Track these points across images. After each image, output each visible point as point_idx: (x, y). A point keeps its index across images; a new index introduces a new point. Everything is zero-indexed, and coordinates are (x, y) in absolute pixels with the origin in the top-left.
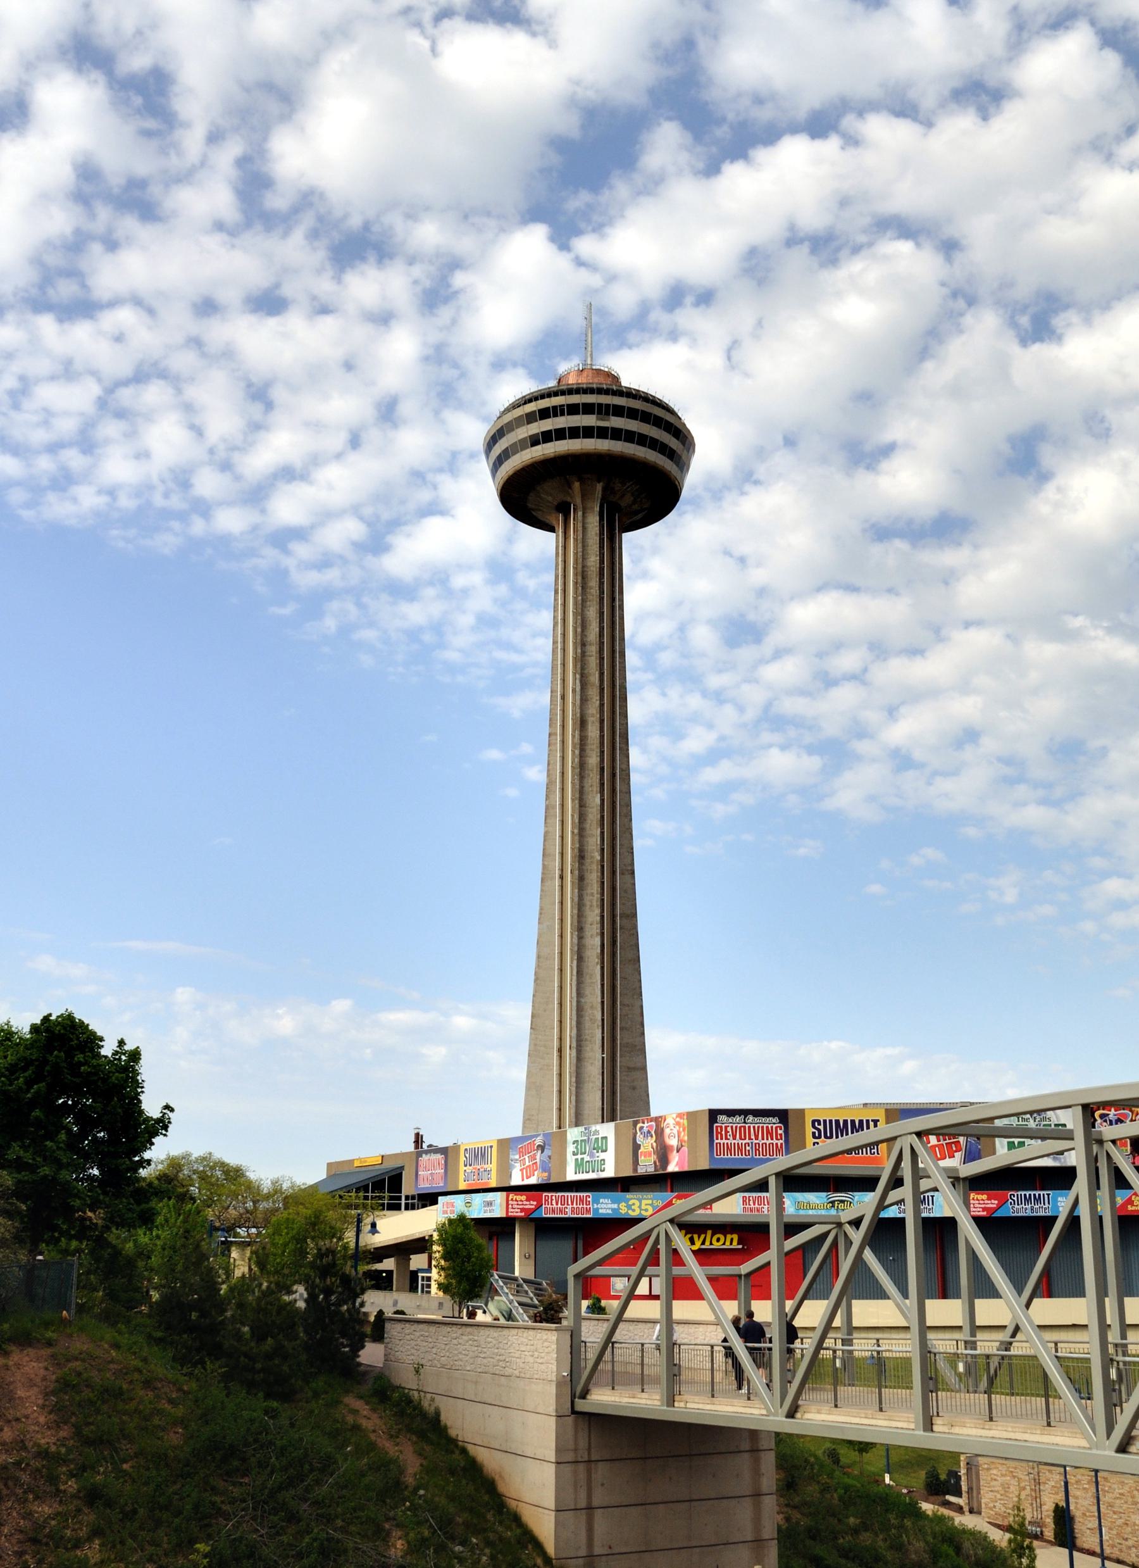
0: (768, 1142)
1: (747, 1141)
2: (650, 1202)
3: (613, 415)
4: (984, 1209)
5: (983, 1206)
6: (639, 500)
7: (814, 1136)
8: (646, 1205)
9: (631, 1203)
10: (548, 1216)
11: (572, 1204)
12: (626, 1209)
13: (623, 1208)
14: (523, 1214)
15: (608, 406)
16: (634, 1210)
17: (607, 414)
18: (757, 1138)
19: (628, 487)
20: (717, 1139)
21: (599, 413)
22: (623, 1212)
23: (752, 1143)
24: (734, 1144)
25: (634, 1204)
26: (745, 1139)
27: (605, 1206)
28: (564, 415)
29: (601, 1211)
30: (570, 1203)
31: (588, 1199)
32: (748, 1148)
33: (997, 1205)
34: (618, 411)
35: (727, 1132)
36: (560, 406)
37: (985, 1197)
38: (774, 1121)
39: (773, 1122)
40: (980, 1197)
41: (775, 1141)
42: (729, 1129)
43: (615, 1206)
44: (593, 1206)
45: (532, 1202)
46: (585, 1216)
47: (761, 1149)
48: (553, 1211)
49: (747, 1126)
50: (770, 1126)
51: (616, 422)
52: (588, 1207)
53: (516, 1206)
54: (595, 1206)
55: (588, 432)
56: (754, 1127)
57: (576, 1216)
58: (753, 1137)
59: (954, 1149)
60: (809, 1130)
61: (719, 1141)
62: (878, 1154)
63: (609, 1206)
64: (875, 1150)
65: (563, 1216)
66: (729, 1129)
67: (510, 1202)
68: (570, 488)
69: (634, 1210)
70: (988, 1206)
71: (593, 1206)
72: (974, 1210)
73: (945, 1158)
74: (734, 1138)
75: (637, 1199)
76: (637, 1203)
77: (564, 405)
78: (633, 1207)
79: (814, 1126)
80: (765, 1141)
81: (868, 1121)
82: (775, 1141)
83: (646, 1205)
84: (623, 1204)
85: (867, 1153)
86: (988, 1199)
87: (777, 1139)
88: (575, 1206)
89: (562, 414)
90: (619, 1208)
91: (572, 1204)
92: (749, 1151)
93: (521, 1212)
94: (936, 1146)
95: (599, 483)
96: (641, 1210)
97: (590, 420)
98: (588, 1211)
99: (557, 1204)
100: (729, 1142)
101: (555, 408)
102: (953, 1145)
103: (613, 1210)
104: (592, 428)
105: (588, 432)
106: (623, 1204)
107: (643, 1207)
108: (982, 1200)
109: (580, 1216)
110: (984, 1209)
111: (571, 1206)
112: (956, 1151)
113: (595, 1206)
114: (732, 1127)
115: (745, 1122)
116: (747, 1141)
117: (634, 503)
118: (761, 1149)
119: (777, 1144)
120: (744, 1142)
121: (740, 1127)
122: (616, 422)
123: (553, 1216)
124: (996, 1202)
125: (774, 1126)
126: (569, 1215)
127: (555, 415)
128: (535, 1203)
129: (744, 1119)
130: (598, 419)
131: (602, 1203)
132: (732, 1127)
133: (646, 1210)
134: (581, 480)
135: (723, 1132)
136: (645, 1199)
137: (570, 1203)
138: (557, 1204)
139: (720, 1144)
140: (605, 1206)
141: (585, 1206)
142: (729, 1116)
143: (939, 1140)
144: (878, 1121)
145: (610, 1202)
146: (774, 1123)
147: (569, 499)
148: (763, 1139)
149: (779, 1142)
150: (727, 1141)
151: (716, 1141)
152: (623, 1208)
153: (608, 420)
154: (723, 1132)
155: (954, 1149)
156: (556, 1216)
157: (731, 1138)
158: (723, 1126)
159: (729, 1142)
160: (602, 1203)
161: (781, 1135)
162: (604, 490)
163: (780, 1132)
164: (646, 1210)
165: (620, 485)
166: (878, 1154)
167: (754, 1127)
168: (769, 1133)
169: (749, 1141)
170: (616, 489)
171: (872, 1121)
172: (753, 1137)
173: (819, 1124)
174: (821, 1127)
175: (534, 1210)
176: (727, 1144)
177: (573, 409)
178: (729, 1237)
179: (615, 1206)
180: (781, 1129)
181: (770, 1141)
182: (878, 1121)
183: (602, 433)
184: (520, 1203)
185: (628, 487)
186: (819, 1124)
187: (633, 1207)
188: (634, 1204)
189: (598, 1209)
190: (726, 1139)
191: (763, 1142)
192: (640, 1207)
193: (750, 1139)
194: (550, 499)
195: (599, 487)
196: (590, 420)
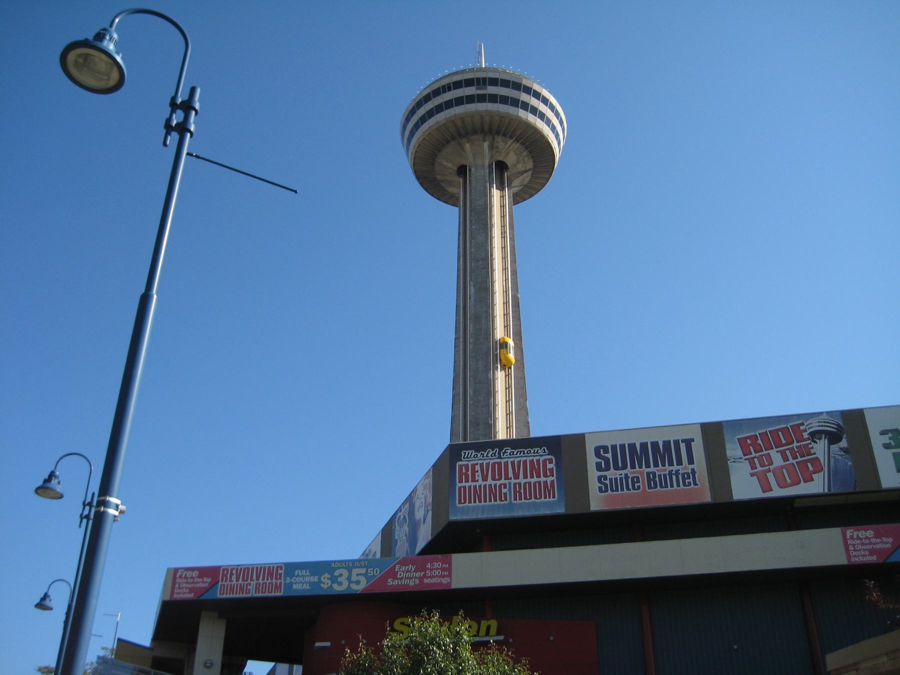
0: (533, 481)
1: (503, 481)
2: (363, 571)
4: (872, 552)
5: (868, 547)
6: (521, 158)
7: (599, 467)
8: (358, 575)
9: (336, 573)
10: (224, 596)
11: (258, 578)
12: (330, 582)
13: (326, 581)
14: (191, 596)
15: (484, 79)
16: (340, 584)
18: (516, 476)
19: (510, 146)
20: (461, 481)
21: (478, 84)
22: (325, 586)
23: (510, 483)
24: (485, 486)
25: (341, 575)
26: (500, 479)
27: (301, 579)
29: (295, 587)
30: (254, 577)
31: (280, 571)
32: (504, 491)
33: (892, 543)
35: (474, 472)
36: (448, 84)
37: (870, 533)
38: (541, 452)
39: (541, 455)
40: (862, 534)
41: (542, 479)
42: (478, 468)
43: (315, 579)
44: (285, 580)
45: (205, 579)
46: (273, 594)
47: (522, 491)
48: (232, 589)
49: (503, 461)
50: (535, 459)
52: (278, 582)
53: (184, 585)
54: (288, 580)
56: (513, 463)
57: (261, 595)
58: (511, 474)
59: (811, 469)
60: (592, 460)
61: (464, 484)
62: (695, 484)
63: (307, 579)
64: (691, 480)
65: (244, 595)
66: (478, 468)
67: (178, 580)
68: (463, 150)
69: (340, 584)
70: (878, 546)
71: (285, 580)
72: (855, 553)
73: (799, 482)
74: (485, 478)
75: (343, 568)
76: (345, 573)
77: (450, 83)
78: (339, 579)
79: (597, 454)
80: (529, 480)
81: (677, 443)
82: (542, 479)
83: (358, 575)
84: (327, 575)
85: (678, 485)
86: (876, 537)
87: (545, 476)
88: (261, 581)
90: (320, 582)
91: (258, 578)
92: (505, 494)
93: (190, 592)
94: (782, 467)
95: (484, 141)
96: (350, 582)
97: (471, 91)
98: (278, 588)
99: (238, 580)
100: (478, 484)
102: (809, 464)
103: (312, 584)
106: (327, 575)
107: (354, 578)
108: (866, 538)
109: (267, 594)
110: (872, 552)
111: (255, 582)
112: (815, 472)
113: (288, 580)
114: (482, 465)
115: (500, 457)
116: (503, 481)
117: (518, 162)
118: (522, 491)
119: (545, 482)
120: (498, 483)
121: (494, 464)
123: (231, 596)
124: (890, 540)
125: (542, 459)
126: (253, 594)
127: (444, 92)
128: (209, 580)
129: (499, 453)
131: (298, 575)
132: (482, 465)
133: (358, 582)
134: (469, 141)
135: (470, 473)
136: (357, 567)
137: (254, 577)
138: (238, 580)
139: (465, 487)
140: (301, 579)
141: (274, 581)
142: (477, 451)
143: (785, 459)
144: (693, 440)
145: (308, 574)
146: (541, 456)
147: (464, 163)
148: (525, 477)
149: (549, 479)
150: (474, 484)
151: (459, 485)
152: (326, 581)
154: (470, 473)
155: (811, 469)
156: (235, 596)
157: (480, 479)
158: (470, 463)
159: (478, 484)
160: (298, 575)
161: (551, 470)
162: (492, 147)
163: (549, 466)
164: (358, 582)
165: (502, 143)
166: (695, 484)
167: (513, 463)
168: (535, 470)
169: (507, 482)
170: (500, 147)
171: (683, 441)
172: (511, 474)
173: (606, 451)
174: (609, 456)
175: (207, 590)
176: (475, 487)
178: (484, 624)
179: (315, 579)
180: (551, 462)
181: (535, 479)
182: (693, 440)
184: (189, 580)
185: (510, 146)
186: (606, 451)
187: (339, 579)
188: (341, 575)
189: (291, 583)
190: (474, 480)
191: (526, 480)
192: (349, 579)
193: (507, 478)
194: (450, 165)
195: (486, 145)
196: (471, 91)
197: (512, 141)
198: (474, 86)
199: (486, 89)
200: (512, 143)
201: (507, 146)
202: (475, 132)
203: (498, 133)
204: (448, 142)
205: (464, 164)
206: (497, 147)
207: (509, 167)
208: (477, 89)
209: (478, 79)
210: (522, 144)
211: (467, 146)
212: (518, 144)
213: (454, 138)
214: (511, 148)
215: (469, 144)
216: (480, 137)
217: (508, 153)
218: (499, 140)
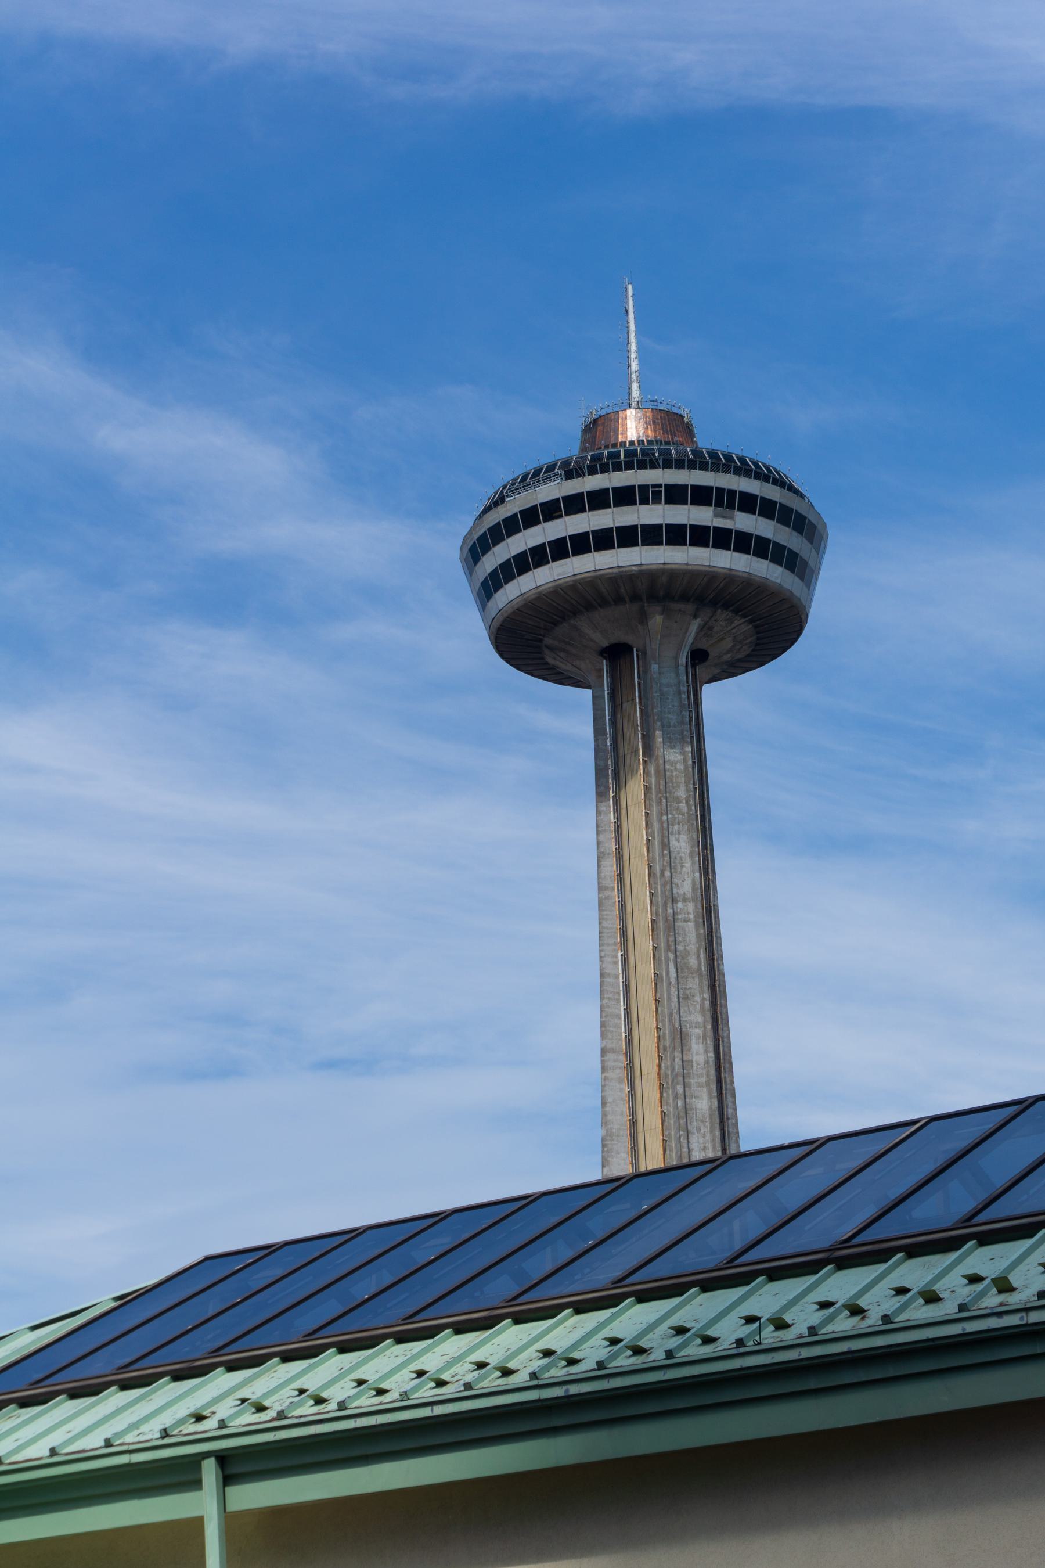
3: (739, 510)
15: (732, 493)
17: (731, 506)
19: (734, 628)
21: (719, 504)
28: (660, 502)
34: (748, 503)
36: (654, 486)
51: (743, 522)
55: (699, 536)
77: (660, 486)
89: (657, 500)
95: (695, 617)
97: (703, 516)
101: (644, 488)
104: (706, 529)
105: (699, 536)
122: (743, 522)
127: (645, 501)
130: (716, 515)
153: (732, 518)
165: (723, 623)
170: (716, 629)
177: (675, 495)
183: (722, 539)
185: (734, 628)
195: (694, 626)
196: (703, 516)
197: (743, 620)
198: (711, 506)
199: (732, 518)
200: (743, 623)
201: (729, 628)
202: (684, 598)
203: (726, 606)
204: (619, 600)
205: (630, 643)
206: (710, 629)
207: (710, 658)
208: (716, 515)
209: (720, 491)
210: (756, 627)
211: (657, 620)
212: (751, 626)
213: (635, 598)
214: (734, 631)
215: (662, 617)
216: (690, 607)
217: (723, 639)
218: (722, 615)
